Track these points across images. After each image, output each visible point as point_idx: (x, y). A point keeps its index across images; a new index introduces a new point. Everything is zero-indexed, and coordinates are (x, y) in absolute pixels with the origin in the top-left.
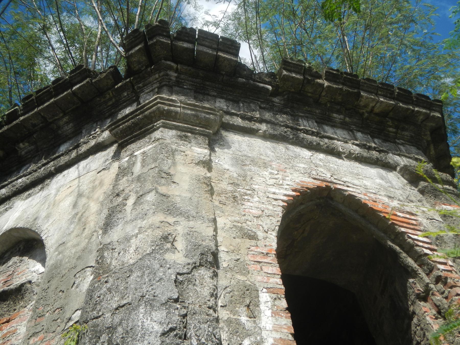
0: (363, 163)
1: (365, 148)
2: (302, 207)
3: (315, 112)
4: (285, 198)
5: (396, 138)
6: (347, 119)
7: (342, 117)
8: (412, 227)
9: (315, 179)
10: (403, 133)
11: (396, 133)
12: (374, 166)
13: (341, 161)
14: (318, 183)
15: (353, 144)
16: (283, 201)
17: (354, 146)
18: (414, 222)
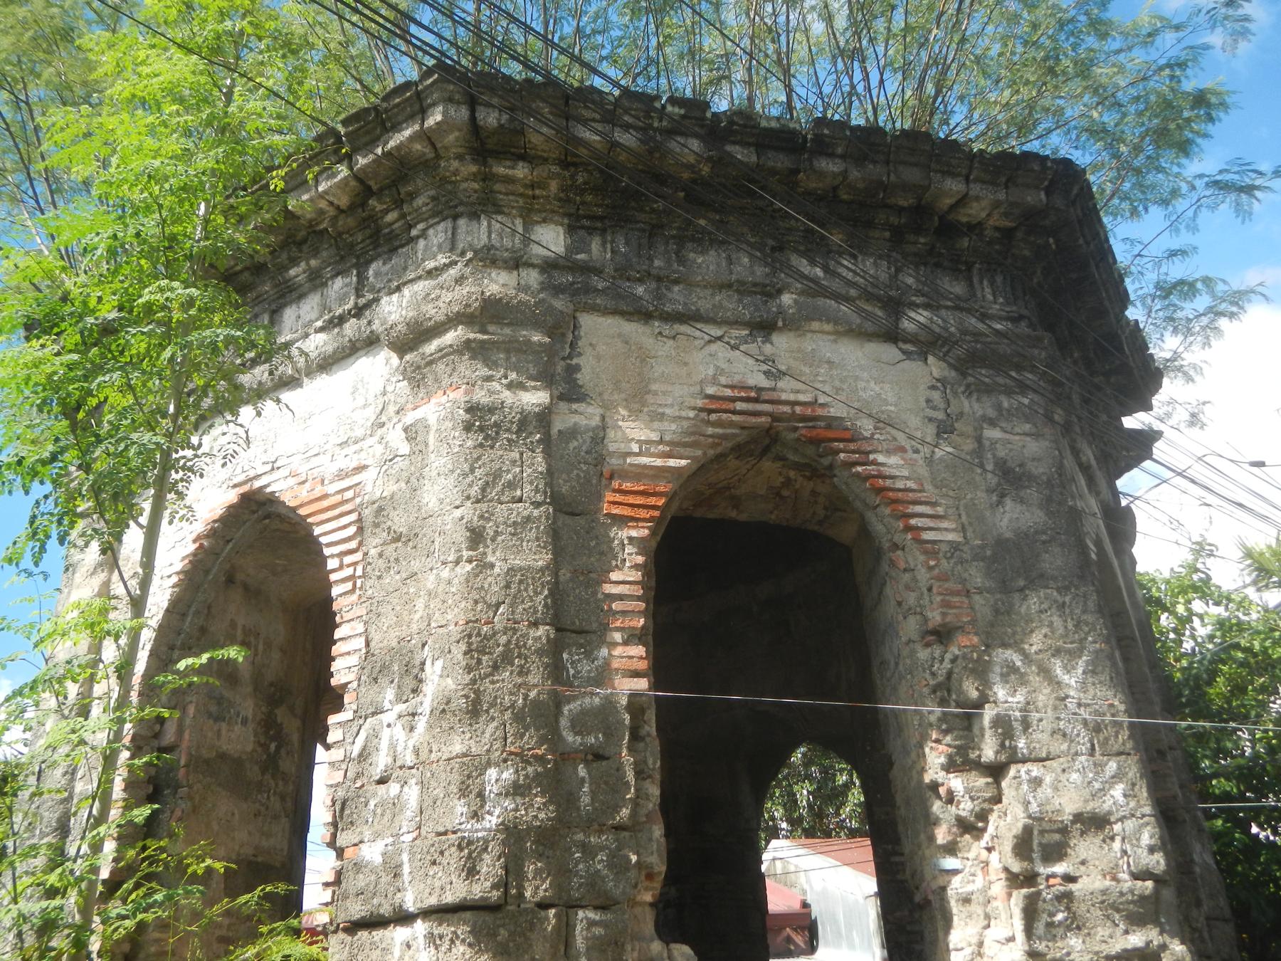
0: (334, 368)
1: (335, 326)
2: (231, 545)
3: (267, 292)
4: (179, 566)
5: (410, 227)
6: (313, 263)
7: (303, 264)
8: (337, 512)
9: (235, 486)
10: (415, 205)
11: (403, 216)
12: (352, 359)
13: (299, 390)
14: (232, 497)
15: (317, 331)
16: (177, 573)
17: (319, 335)
18: (349, 494)
